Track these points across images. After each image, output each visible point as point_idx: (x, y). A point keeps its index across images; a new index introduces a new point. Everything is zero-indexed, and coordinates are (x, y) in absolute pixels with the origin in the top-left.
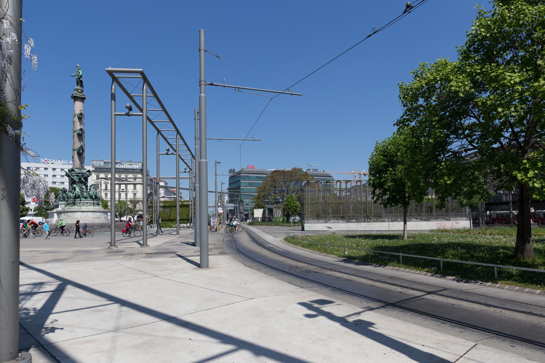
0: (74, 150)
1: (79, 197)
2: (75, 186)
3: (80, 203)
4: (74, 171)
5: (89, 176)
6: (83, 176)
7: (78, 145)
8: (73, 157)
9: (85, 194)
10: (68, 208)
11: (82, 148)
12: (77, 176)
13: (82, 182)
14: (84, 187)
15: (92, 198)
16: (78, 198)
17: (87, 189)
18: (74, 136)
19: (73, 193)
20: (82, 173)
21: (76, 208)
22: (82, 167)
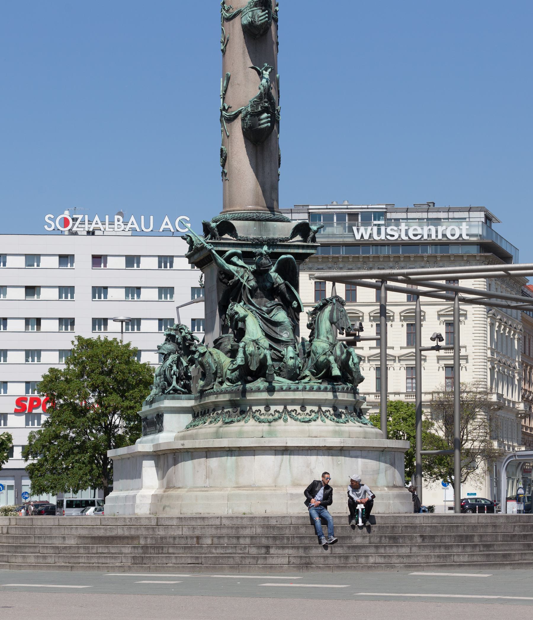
0: (230, 120)
1: (262, 371)
2: (239, 309)
3: (267, 405)
4: (232, 230)
5: (301, 257)
6: (274, 256)
7: (247, 89)
8: (224, 158)
9: (289, 352)
10: (207, 433)
11: (268, 102)
12: (246, 256)
13: (272, 292)
14: (281, 316)
15: (328, 378)
17: (296, 329)
18: (226, 42)
19: (233, 353)
20: (271, 243)
21: (247, 431)
22: (271, 210)
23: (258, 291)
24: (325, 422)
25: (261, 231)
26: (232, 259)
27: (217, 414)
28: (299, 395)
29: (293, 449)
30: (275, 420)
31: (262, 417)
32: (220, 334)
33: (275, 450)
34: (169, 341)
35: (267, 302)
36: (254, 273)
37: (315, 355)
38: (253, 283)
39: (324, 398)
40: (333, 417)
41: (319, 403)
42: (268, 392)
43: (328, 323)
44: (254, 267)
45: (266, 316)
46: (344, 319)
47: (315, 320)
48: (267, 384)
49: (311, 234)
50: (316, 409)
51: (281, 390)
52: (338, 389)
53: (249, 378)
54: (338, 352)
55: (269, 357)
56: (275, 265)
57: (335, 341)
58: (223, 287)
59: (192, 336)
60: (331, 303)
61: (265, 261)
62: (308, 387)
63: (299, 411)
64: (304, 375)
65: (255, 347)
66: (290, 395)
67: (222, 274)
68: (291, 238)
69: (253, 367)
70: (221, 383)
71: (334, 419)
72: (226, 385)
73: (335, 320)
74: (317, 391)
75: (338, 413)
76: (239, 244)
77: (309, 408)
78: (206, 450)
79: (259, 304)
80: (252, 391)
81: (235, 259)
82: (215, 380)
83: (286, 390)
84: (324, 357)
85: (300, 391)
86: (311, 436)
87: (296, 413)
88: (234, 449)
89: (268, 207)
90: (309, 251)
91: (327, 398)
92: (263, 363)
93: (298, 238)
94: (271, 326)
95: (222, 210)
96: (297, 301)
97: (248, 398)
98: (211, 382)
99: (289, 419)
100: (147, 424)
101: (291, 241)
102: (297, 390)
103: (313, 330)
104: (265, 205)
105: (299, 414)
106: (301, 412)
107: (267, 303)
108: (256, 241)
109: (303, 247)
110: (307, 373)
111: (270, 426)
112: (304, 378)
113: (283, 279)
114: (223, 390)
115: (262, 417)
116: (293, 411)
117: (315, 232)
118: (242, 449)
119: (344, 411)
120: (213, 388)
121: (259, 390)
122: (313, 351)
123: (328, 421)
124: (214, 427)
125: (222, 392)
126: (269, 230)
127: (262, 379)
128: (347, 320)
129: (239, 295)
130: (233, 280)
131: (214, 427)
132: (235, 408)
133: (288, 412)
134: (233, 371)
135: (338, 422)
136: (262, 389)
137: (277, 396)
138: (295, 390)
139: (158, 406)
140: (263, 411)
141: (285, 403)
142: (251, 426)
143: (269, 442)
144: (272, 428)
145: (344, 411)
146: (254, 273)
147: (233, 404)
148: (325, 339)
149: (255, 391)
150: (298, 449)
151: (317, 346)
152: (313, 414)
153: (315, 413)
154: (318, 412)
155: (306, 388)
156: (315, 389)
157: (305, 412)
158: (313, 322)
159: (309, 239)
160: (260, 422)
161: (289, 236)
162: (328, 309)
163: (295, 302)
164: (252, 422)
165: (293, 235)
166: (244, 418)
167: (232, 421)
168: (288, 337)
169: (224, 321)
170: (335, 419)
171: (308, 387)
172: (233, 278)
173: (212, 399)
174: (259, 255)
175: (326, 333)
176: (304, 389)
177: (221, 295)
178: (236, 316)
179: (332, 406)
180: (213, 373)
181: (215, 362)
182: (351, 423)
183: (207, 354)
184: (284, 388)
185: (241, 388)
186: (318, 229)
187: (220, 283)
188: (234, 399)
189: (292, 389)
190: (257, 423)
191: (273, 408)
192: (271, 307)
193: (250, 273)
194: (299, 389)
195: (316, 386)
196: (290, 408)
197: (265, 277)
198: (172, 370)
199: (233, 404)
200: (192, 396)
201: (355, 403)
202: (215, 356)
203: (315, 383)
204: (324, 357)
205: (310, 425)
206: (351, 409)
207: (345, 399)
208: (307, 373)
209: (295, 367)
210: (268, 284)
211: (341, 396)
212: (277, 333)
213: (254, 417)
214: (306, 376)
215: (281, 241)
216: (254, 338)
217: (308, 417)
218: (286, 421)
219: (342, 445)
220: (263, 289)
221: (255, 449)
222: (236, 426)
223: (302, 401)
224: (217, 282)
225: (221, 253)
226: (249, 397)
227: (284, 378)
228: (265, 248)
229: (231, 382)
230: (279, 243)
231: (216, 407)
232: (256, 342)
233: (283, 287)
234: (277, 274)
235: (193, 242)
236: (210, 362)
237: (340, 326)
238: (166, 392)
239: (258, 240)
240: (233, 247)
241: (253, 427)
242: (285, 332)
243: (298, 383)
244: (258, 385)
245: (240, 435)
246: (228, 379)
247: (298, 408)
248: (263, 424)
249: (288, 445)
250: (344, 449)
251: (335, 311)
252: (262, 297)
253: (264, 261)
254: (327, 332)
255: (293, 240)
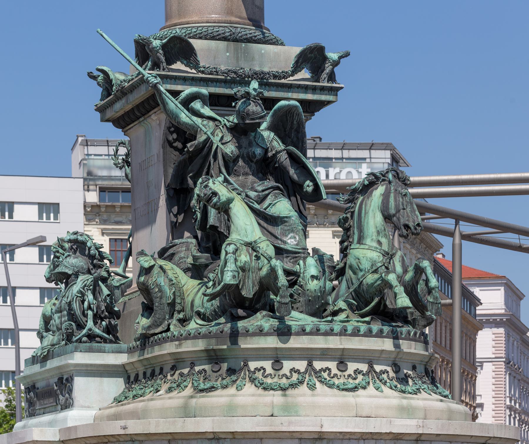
5: (311, 107)
16: (252, 307)
20: (264, 79)
23: (241, 163)
24: (382, 392)
25: (237, 59)
26: (192, 104)
27: (181, 375)
28: (334, 343)
29: (332, 436)
30: (293, 386)
31: (269, 381)
32: (168, 239)
33: (300, 439)
34: (75, 253)
35: (255, 182)
36: (234, 130)
37: (355, 273)
38: (230, 149)
39: (380, 348)
40: (395, 383)
41: (370, 358)
42: (278, 335)
43: (379, 218)
44: (233, 119)
45: (256, 206)
46: (408, 210)
47: (353, 213)
48: (275, 323)
49: (328, 68)
50: (364, 367)
51: (303, 332)
52: (401, 333)
53: (241, 312)
54: (399, 269)
55: (280, 272)
56: (268, 118)
57: (392, 249)
58: (175, 157)
59: (99, 252)
60: (384, 180)
61: (255, 108)
62: (350, 329)
63: (335, 371)
64: (336, 308)
65: (251, 255)
66: (319, 343)
67: (172, 133)
68: (294, 73)
69: (248, 291)
70: (183, 322)
71: (396, 387)
72: (193, 325)
73: (392, 211)
74: (365, 335)
75: (402, 376)
76: (201, 80)
77: (352, 367)
78: (170, 437)
79: (243, 186)
80: (247, 333)
81: (197, 105)
82: (171, 317)
83: (311, 333)
84: (376, 276)
85: (336, 335)
86: (359, 414)
87: (329, 375)
88: (223, 436)
89: (250, 19)
90: (323, 98)
91: (383, 348)
92: (267, 285)
93: (305, 74)
94: (265, 225)
95: (163, 25)
96: (314, 180)
97: (243, 346)
98: (164, 319)
99: (318, 385)
100: (36, 395)
101: (291, 78)
102: (330, 333)
103: (347, 230)
104: (244, 15)
105: (335, 375)
106: (339, 373)
107: (256, 185)
108: (233, 75)
109: (314, 89)
110: (341, 304)
111: (285, 395)
112: (335, 313)
113: (283, 143)
114: (193, 332)
115: (269, 381)
116: (325, 371)
117: (336, 64)
118: (237, 437)
119: (410, 372)
120: (168, 330)
121: (260, 332)
122: (351, 267)
123: (386, 390)
124: (179, 398)
125: (189, 337)
126: (253, 59)
127: (264, 313)
128: (415, 211)
129: (205, 170)
130: (196, 142)
131: (179, 398)
132: (217, 363)
133: (316, 372)
134: (213, 297)
135: (403, 392)
136: (266, 329)
137: (295, 343)
138: (326, 334)
139: (63, 363)
140: (269, 370)
141: (309, 356)
142: (249, 395)
143: (290, 423)
144: (290, 399)
145: (410, 372)
146: (234, 130)
147: (214, 357)
148: (375, 244)
149: (254, 334)
150: (341, 437)
151: (361, 256)
152: (360, 377)
153: (363, 375)
154: (368, 373)
155: (346, 330)
156: (362, 333)
157: (346, 373)
158: (349, 215)
159: (324, 75)
160: (265, 389)
161: (289, 68)
162: (379, 191)
163: (308, 182)
164: (249, 388)
165: (297, 68)
166: (234, 382)
167: (213, 387)
168: (297, 245)
169: (176, 216)
170: (399, 386)
171: (350, 329)
172: (195, 138)
173: (170, 348)
174: (242, 97)
175: (375, 234)
176: (343, 333)
177: (171, 171)
178: (215, 200)
179: (390, 363)
180: (169, 304)
181: (172, 284)
182: (424, 395)
183: (156, 270)
184: (308, 329)
185: (227, 328)
186: (340, 58)
187: (169, 149)
188: (215, 347)
189: (322, 331)
190: (260, 391)
191: (287, 365)
192: (263, 191)
193: (225, 130)
194: (335, 331)
195: (363, 328)
196: (318, 365)
197: (251, 138)
198: (83, 302)
199: (214, 357)
200: (124, 346)
201: (426, 360)
202: (170, 274)
203: (355, 322)
204: (376, 276)
205: (358, 396)
206: (421, 369)
207: (413, 351)
208: (341, 304)
209: (323, 293)
210: (258, 151)
211: (407, 347)
212: (276, 238)
213: (252, 380)
214: (341, 310)
215: (275, 77)
216: (248, 240)
217: (350, 380)
218: (312, 387)
219: (421, 432)
220: (249, 159)
221: (262, 436)
222: (222, 396)
223: (340, 353)
224: (163, 147)
225: (175, 94)
226: (245, 344)
227: (301, 312)
228: (255, 84)
229: (203, 319)
230: (273, 81)
231: (177, 362)
232: (252, 246)
233: (283, 157)
234: (272, 134)
235: (111, 81)
236: (163, 284)
237: (402, 221)
238: (74, 339)
239: (235, 73)
240: (191, 85)
241: (254, 398)
242: (291, 235)
243: (331, 321)
244: (259, 323)
245: (230, 410)
246: (199, 314)
247: (332, 365)
248: (272, 392)
249: (324, 430)
250: (423, 438)
251: (392, 195)
252: (246, 174)
253: (254, 108)
254: (378, 233)
255: (296, 77)
